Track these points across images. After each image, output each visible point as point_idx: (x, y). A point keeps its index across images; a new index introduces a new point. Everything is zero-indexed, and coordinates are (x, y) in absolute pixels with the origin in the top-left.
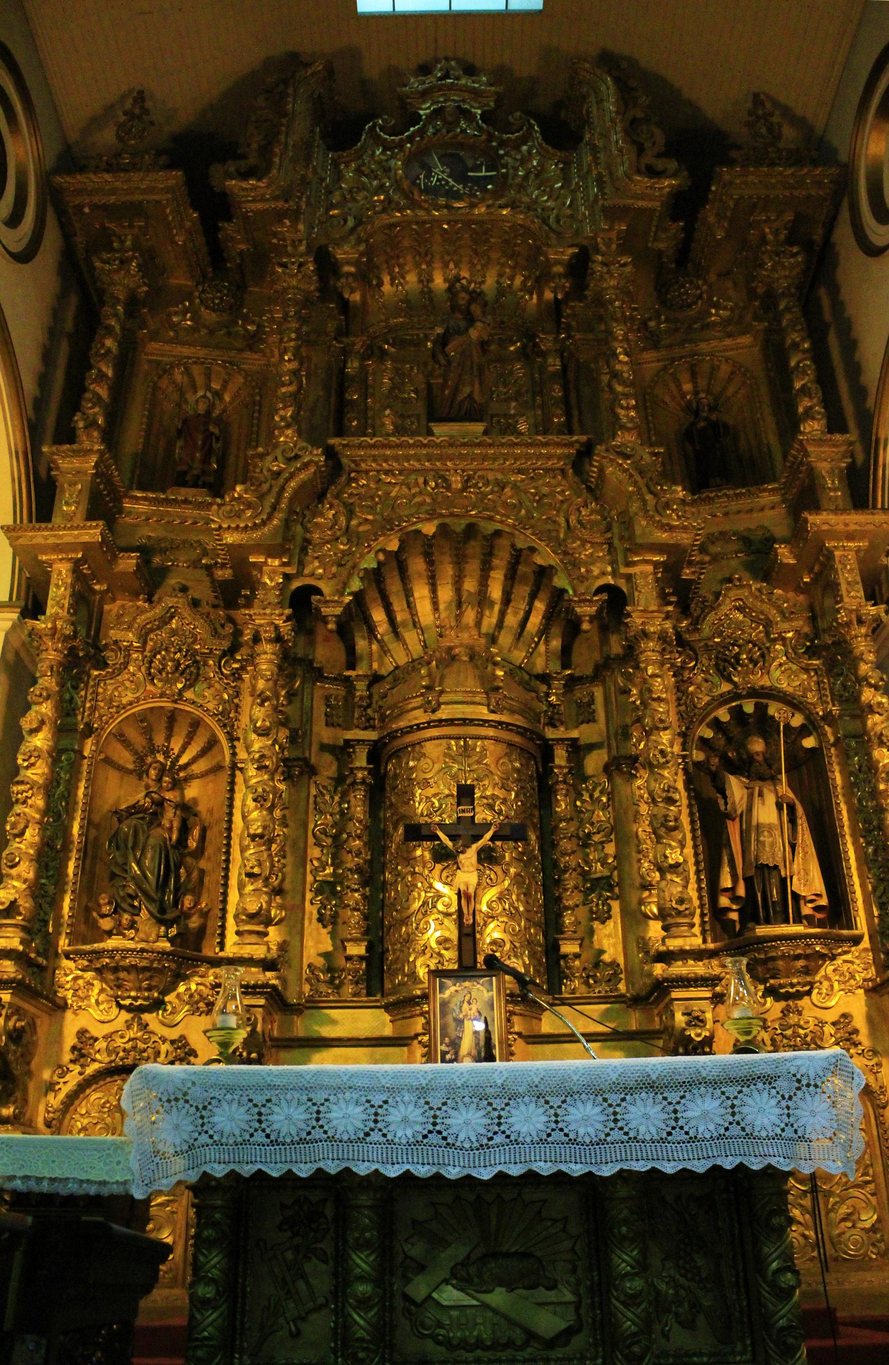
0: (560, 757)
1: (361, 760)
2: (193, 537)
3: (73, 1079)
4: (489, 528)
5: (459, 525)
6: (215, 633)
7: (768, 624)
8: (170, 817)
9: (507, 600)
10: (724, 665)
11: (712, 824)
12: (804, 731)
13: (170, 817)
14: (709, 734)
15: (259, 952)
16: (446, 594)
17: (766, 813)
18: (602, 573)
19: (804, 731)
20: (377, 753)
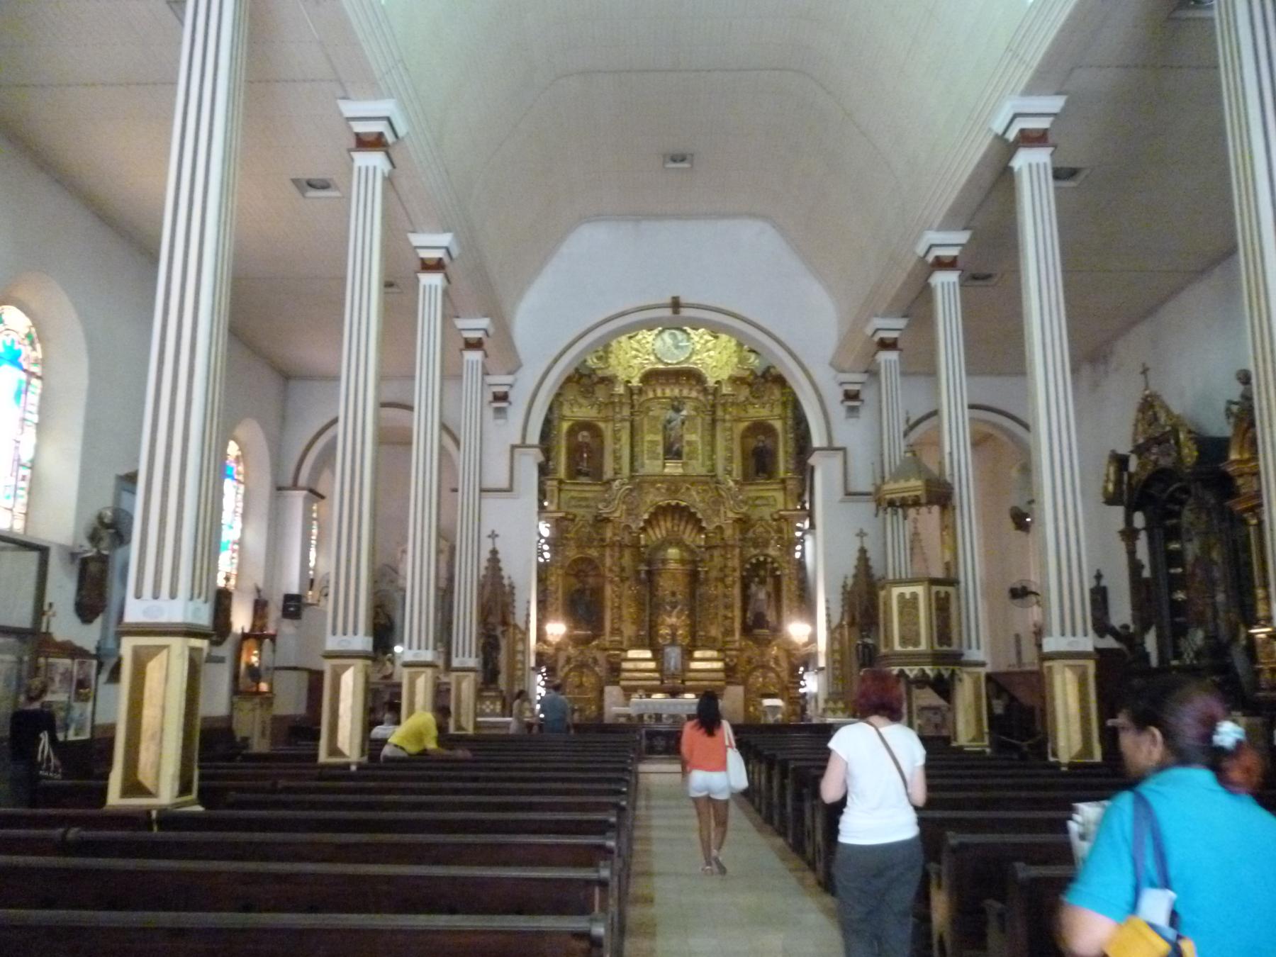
0: (702, 576)
1: (643, 576)
2: (587, 495)
3: (566, 669)
4: (683, 504)
5: (673, 503)
6: (598, 533)
7: (768, 532)
8: (588, 592)
9: (687, 523)
10: (756, 546)
11: (746, 598)
12: (776, 569)
13: (588, 592)
14: (748, 566)
15: (617, 638)
16: (669, 519)
17: (762, 595)
18: (717, 522)
19: (776, 569)
20: (649, 573)
